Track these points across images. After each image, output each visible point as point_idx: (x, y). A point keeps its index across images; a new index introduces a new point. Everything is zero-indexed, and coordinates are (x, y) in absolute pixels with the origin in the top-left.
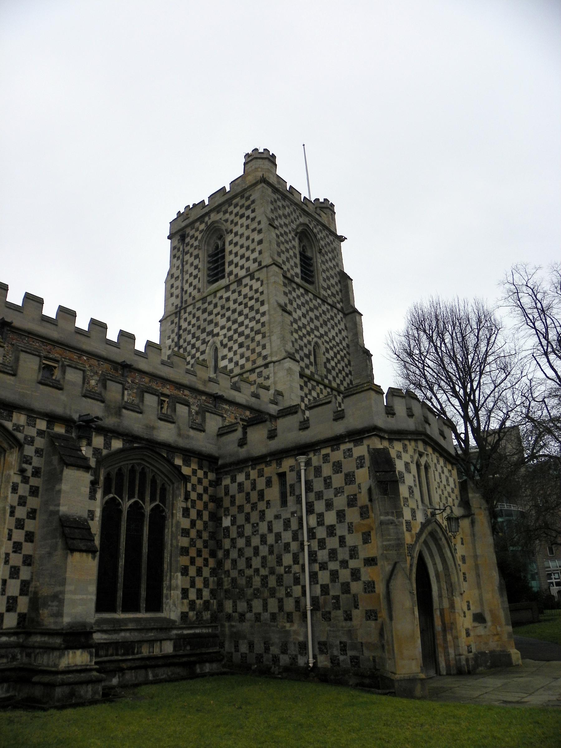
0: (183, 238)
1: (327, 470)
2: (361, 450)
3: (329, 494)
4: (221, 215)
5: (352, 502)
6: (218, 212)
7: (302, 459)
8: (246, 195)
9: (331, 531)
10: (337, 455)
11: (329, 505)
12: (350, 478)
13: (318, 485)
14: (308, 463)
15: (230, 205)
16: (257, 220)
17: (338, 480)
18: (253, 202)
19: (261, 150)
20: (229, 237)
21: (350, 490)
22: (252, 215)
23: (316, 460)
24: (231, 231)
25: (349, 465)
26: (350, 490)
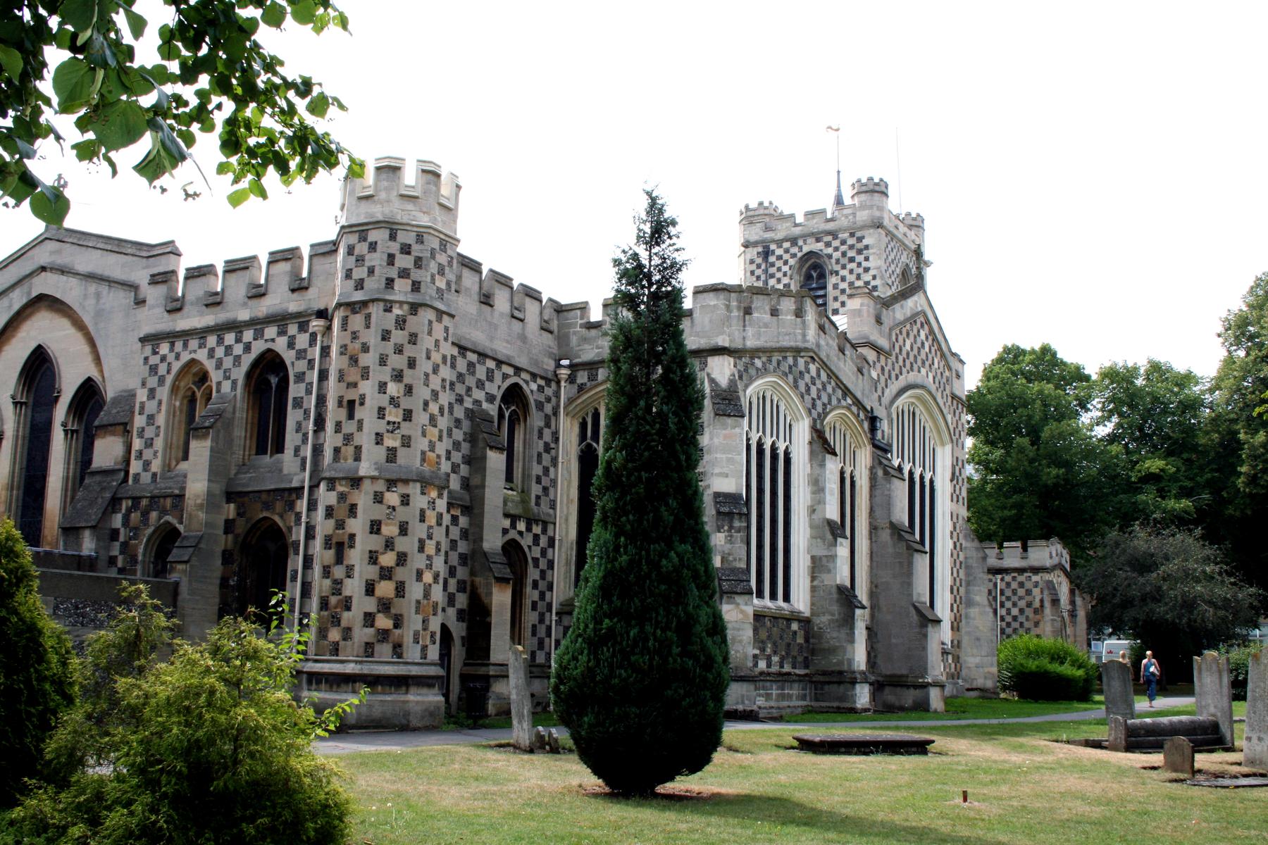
0: (766, 253)
1: (1014, 585)
2: (1035, 578)
3: (1015, 598)
4: (820, 246)
5: (1029, 605)
6: (818, 240)
7: (999, 577)
8: (858, 234)
9: (1015, 618)
10: (1021, 578)
11: (1015, 605)
12: (1029, 592)
13: (1008, 593)
14: (1002, 580)
15: (835, 237)
16: (872, 272)
17: (1021, 592)
18: (867, 247)
19: (876, 180)
20: (832, 280)
21: (1028, 598)
22: (865, 264)
23: (1008, 578)
24: (837, 273)
25: (1028, 585)
26: (1028, 598)
